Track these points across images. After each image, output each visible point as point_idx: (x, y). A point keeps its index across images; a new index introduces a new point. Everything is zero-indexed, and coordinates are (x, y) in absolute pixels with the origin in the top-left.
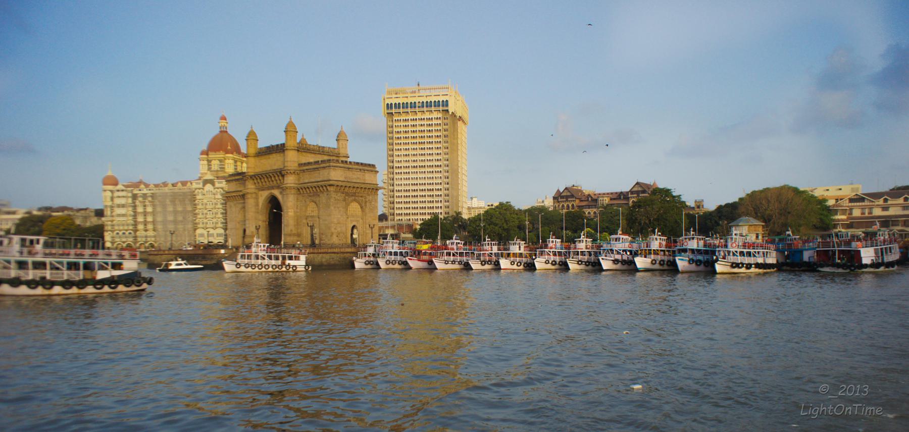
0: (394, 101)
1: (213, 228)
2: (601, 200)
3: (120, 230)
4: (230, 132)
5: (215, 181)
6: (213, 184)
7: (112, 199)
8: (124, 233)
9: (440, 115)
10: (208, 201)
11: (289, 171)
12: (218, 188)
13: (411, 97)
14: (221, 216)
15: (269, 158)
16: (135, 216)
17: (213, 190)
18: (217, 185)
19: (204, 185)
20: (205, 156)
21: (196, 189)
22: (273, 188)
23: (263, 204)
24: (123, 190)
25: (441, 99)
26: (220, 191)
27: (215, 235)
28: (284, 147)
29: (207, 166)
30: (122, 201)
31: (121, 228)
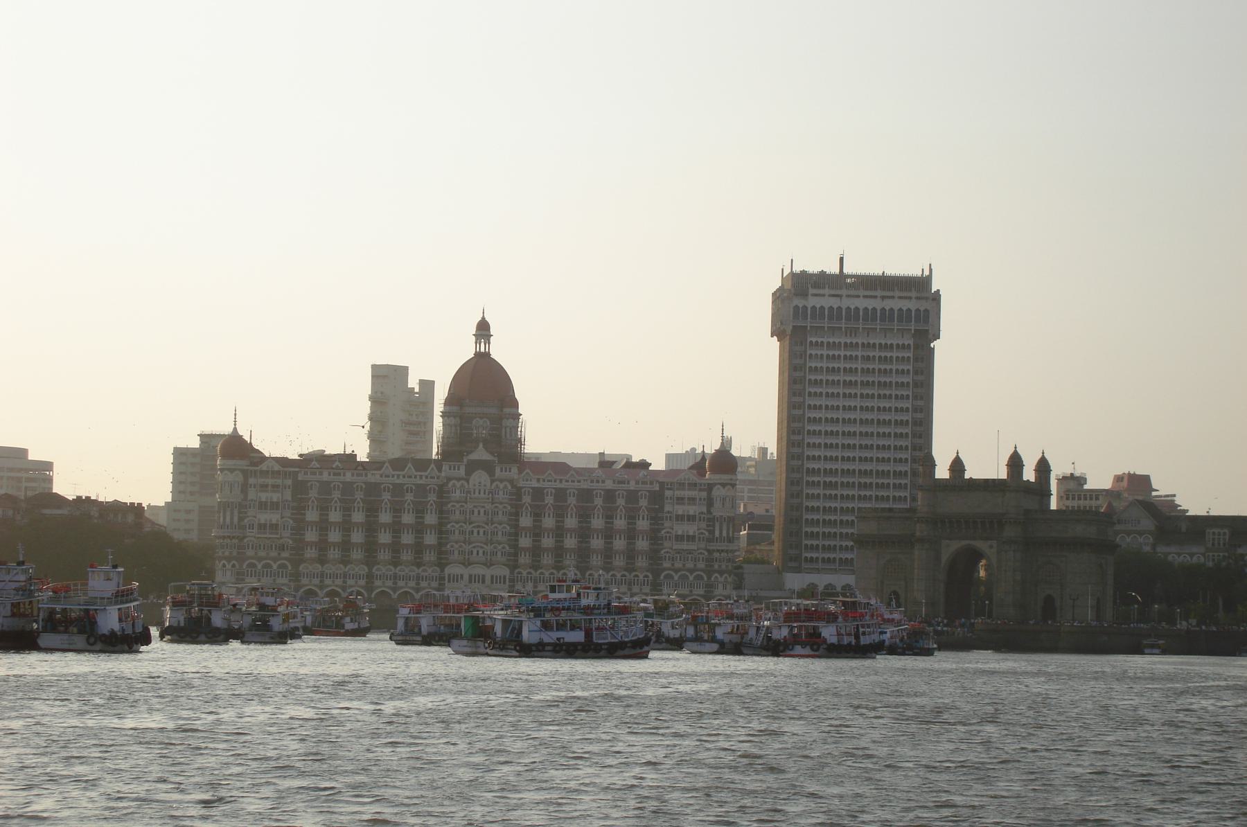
0: (812, 302)
1: (485, 564)
2: (1214, 533)
3: (260, 560)
4: (494, 355)
6: (491, 472)
7: (245, 488)
8: (267, 566)
9: (908, 341)
10: (475, 507)
12: (501, 481)
13: (848, 296)
16: (300, 526)
17: (488, 484)
19: (469, 472)
21: (449, 479)
24: (273, 472)
25: (912, 305)
26: (505, 487)
27: (488, 579)
29: (458, 428)
30: (275, 497)
31: (262, 554)
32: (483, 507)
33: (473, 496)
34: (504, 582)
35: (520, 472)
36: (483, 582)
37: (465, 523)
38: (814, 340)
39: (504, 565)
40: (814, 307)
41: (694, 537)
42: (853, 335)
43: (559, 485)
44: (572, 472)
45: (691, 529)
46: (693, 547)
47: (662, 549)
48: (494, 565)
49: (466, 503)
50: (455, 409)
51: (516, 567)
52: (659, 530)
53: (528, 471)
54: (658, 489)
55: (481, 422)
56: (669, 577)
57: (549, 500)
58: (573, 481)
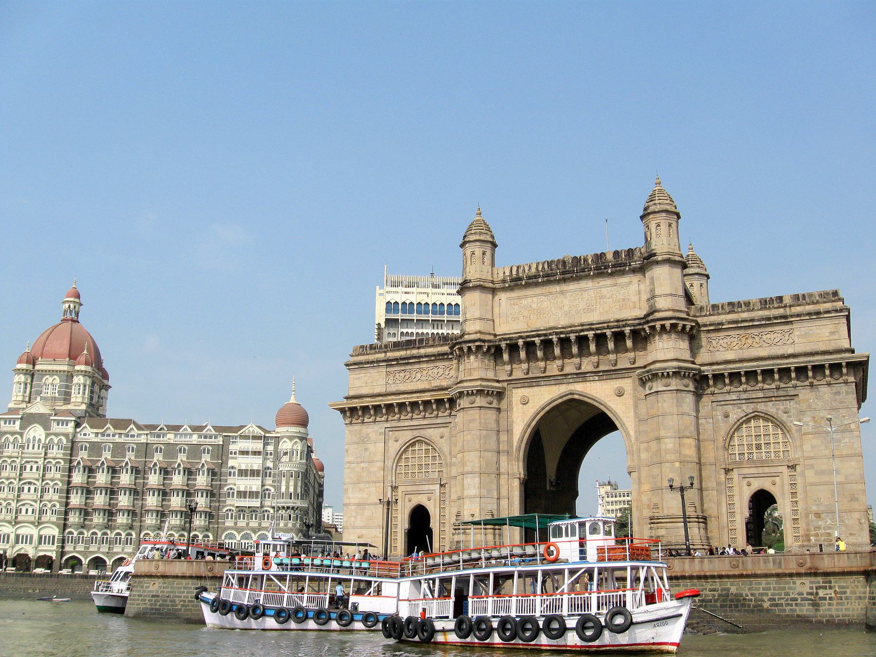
0: (400, 298)
1: (33, 523)
5: (51, 418)
6: (46, 425)
10: (28, 462)
11: (681, 323)
12: (57, 435)
14: (56, 497)
15: (562, 292)
18: (55, 428)
19: (23, 427)
20: (30, 367)
22: (581, 376)
23: (529, 425)
28: (654, 255)
29: (29, 386)
32: (36, 462)
33: (26, 450)
34: (53, 544)
35: (78, 425)
36: (31, 543)
37: (15, 479)
38: (405, 331)
39: (53, 523)
40: (404, 303)
41: (257, 493)
42: (440, 327)
43: (117, 439)
44: (132, 426)
45: (254, 484)
46: (256, 503)
47: (224, 507)
48: (43, 523)
49: (17, 458)
50: (24, 366)
51: (65, 526)
52: (221, 487)
53: (85, 425)
54: (221, 443)
55: (51, 379)
56: (230, 536)
57: (107, 455)
58: (133, 436)
